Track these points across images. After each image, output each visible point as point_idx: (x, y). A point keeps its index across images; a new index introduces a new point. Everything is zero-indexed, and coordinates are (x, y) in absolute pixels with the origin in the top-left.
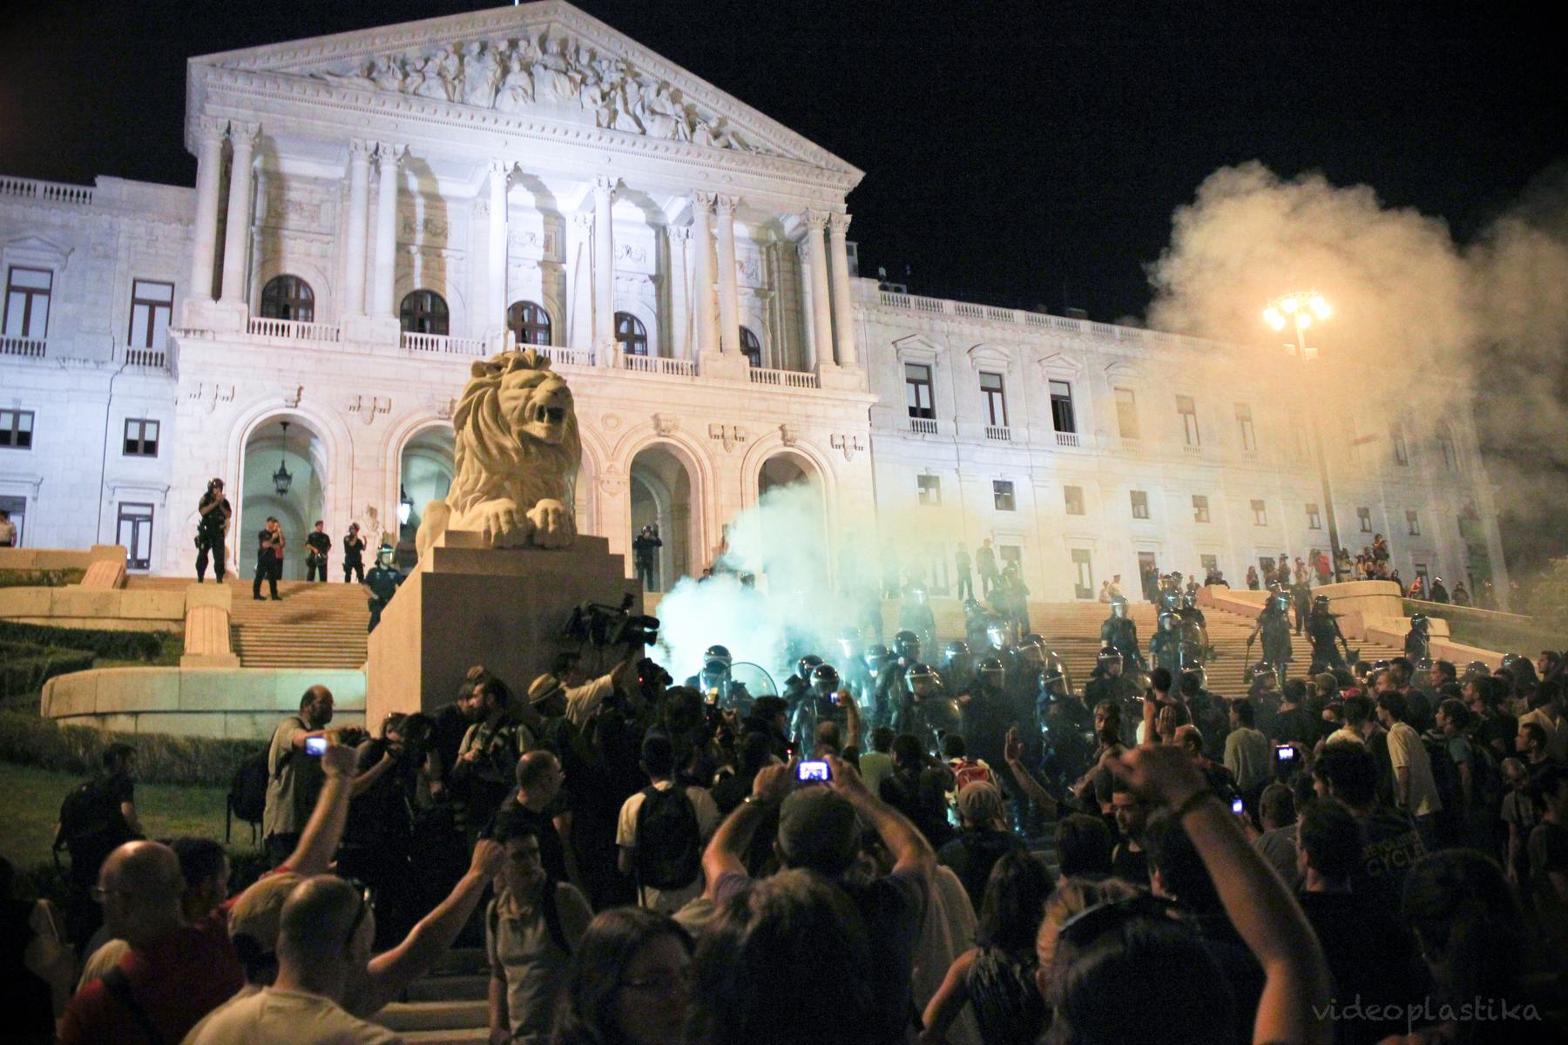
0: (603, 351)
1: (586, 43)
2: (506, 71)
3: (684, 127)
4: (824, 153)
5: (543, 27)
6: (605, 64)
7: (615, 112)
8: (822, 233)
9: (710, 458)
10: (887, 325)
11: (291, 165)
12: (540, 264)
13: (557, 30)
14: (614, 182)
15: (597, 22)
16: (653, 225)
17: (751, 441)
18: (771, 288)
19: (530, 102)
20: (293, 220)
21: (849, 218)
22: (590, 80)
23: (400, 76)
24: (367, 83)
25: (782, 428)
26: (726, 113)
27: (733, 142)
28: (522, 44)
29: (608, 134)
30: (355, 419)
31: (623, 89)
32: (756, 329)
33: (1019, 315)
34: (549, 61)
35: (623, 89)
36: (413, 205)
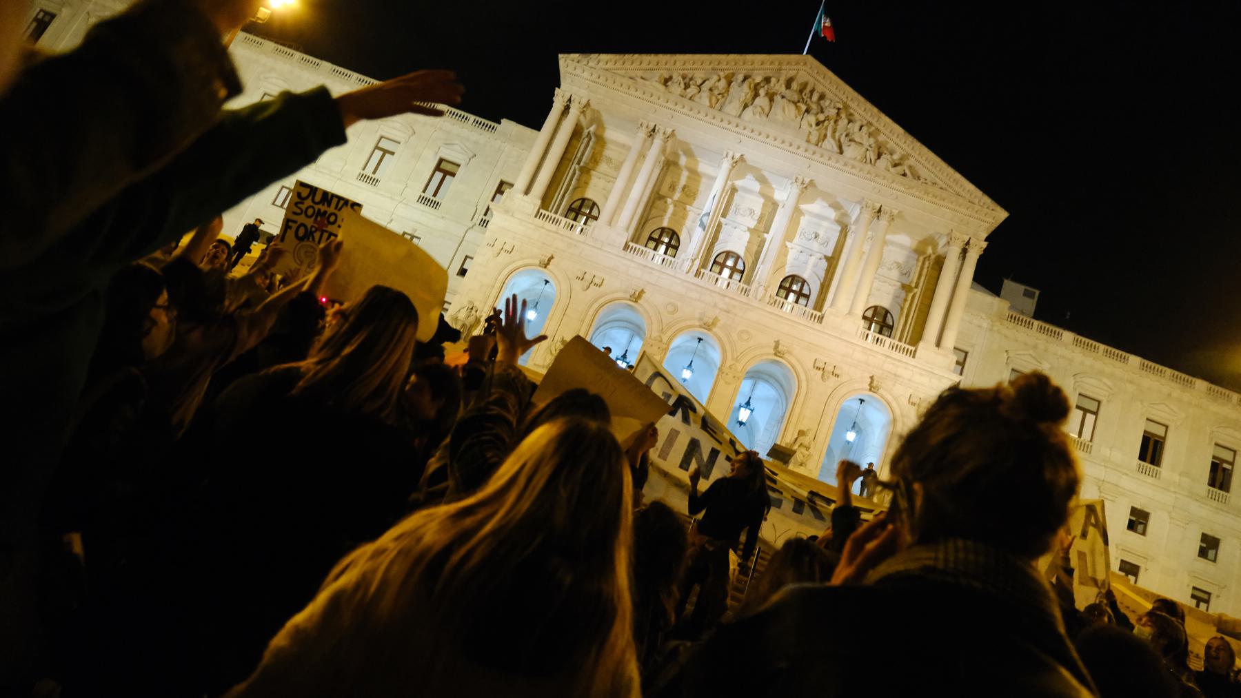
0: (757, 290)
1: (820, 88)
2: (756, 95)
3: (872, 155)
4: (979, 193)
5: (792, 73)
6: (828, 102)
7: (825, 136)
8: (959, 250)
9: (807, 381)
10: (1006, 337)
11: (611, 134)
12: (749, 229)
13: (802, 77)
14: (807, 180)
15: (830, 74)
16: (839, 222)
17: (843, 378)
18: (917, 287)
19: (764, 117)
20: (603, 167)
21: (985, 245)
22: (814, 111)
23: (682, 85)
24: (662, 87)
25: (872, 378)
26: (910, 152)
27: (907, 172)
28: (773, 80)
29: (813, 148)
30: (578, 285)
31: (836, 121)
32: (895, 312)
33: (1135, 360)
34: (788, 93)
35: (836, 121)
36: (679, 175)
